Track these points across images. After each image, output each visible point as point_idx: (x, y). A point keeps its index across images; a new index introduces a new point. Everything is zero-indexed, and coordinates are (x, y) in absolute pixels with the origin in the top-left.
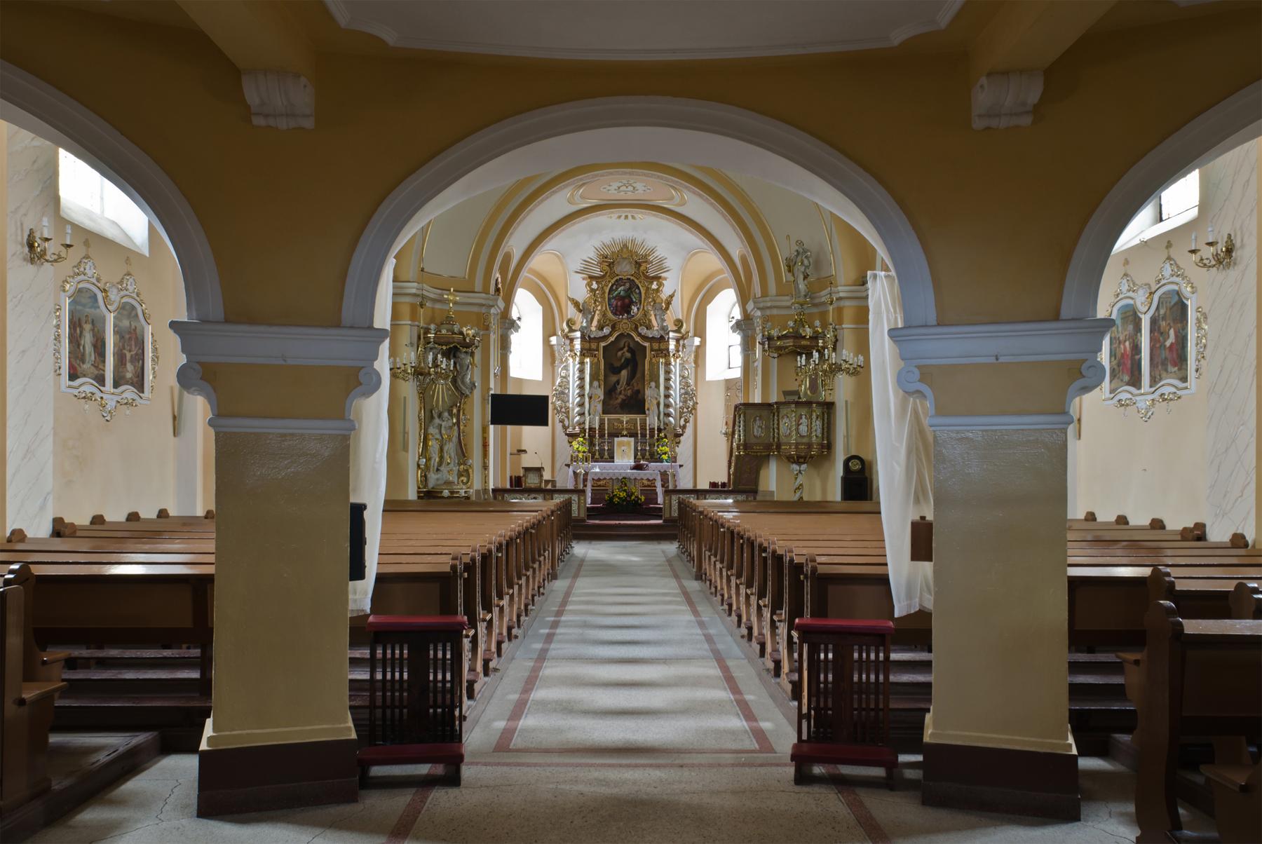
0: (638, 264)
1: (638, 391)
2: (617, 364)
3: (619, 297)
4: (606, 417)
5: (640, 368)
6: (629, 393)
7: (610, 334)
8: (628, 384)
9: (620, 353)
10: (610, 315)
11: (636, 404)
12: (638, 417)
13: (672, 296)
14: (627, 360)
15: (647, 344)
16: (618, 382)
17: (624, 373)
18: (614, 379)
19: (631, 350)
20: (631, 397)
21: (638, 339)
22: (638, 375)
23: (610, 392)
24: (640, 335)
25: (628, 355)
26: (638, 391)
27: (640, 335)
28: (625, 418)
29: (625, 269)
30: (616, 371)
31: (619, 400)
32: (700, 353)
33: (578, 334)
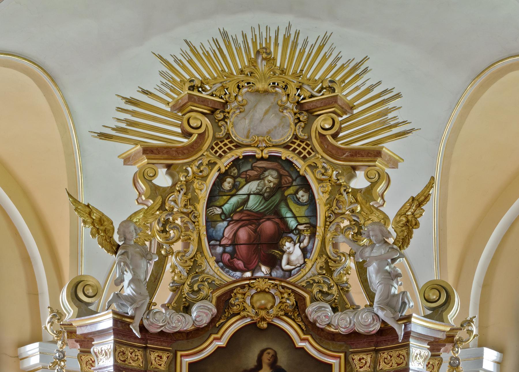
0: (306, 111)
13: (419, 201)
24: (311, 328)
27: (311, 328)
33: (105, 321)
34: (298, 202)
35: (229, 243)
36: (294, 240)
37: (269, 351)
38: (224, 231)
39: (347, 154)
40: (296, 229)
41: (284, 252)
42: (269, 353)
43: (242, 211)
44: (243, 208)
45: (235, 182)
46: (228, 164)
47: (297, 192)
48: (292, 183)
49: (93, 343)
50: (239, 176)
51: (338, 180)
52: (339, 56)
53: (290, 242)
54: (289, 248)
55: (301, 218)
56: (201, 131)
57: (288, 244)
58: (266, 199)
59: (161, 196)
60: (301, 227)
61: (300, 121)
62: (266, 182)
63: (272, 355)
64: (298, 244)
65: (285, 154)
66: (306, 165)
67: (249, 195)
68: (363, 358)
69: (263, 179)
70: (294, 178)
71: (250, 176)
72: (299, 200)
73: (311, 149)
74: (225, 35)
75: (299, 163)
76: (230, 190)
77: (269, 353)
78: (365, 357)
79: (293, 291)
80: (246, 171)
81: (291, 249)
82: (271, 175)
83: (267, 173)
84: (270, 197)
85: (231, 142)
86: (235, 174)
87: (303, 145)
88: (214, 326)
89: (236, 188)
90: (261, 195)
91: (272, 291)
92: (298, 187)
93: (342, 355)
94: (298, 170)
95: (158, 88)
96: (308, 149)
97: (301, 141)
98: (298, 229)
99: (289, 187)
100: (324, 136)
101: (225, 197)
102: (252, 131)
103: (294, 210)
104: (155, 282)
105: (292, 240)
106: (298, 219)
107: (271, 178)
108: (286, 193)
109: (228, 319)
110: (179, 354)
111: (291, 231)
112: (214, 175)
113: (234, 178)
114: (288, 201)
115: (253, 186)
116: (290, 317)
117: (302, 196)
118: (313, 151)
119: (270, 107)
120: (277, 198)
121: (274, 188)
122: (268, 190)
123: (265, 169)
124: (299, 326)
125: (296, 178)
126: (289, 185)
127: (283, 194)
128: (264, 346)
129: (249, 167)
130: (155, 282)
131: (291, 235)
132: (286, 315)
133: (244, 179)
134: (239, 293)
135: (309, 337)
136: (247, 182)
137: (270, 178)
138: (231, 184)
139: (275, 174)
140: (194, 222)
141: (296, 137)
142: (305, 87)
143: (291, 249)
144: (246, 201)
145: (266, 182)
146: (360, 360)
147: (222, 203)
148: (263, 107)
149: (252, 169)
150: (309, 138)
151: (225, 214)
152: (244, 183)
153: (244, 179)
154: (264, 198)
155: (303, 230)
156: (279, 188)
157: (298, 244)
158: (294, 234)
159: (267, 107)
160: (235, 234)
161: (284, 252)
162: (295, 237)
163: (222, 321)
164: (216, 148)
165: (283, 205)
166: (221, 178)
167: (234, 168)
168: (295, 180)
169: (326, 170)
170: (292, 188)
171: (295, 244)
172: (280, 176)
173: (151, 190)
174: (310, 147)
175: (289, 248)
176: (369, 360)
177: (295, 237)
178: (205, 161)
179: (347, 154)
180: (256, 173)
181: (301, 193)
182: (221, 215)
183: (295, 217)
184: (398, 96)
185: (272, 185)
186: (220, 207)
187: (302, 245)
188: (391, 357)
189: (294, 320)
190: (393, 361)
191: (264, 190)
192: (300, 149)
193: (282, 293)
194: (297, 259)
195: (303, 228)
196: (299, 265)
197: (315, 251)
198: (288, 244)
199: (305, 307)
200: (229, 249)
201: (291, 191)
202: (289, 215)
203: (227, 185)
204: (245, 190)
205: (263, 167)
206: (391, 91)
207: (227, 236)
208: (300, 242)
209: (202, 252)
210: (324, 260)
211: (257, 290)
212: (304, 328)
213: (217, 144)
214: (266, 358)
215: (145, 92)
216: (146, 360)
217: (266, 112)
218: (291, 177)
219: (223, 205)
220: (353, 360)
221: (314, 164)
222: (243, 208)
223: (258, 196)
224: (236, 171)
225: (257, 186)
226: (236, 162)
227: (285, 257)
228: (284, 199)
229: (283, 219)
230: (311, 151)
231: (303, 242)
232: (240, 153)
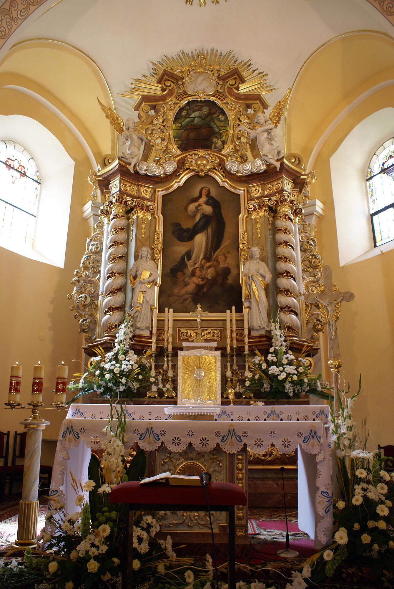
0: (223, 79)
1: (227, 271)
2: (188, 225)
3: (191, 128)
4: (170, 315)
5: (228, 230)
6: (210, 273)
7: (175, 174)
8: (208, 258)
9: (192, 207)
10: (175, 150)
11: (225, 293)
12: (230, 316)
14: (204, 216)
15: (241, 191)
16: (189, 255)
17: (200, 239)
18: (181, 249)
19: (212, 202)
20: (213, 282)
21: (226, 184)
22: (226, 242)
23: (173, 272)
24: (228, 174)
25: (208, 209)
26: (227, 271)
27: (228, 174)
28: (199, 314)
29: (202, 88)
30: (187, 235)
31: (191, 287)
32: (328, 220)
34: (219, 120)
41: (212, 143)
47: (219, 116)
50: (190, 109)
56: (170, 88)
57: (214, 139)
58: (203, 119)
60: (221, 132)
65: (212, 99)
67: (195, 117)
69: (202, 111)
74: (183, 52)
75: (219, 103)
79: (218, 156)
83: (203, 108)
89: (188, 115)
91: (207, 157)
93: (245, 189)
99: (214, 114)
107: (206, 110)
108: (213, 117)
109: (184, 171)
110: (157, 190)
111: (216, 133)
112: (177, 109)
113: (187, 110)
115: (197, 114)
116: (216, 170)
120: (209, 118)
123: (203, 106)
127: (212, 117)
128: (203, 186)
132: (214, 169)
136: (194, 112)
137: (205, 110)
139: (208, 108)
141: (218, 92)
142: (221, 70)
144: (193, 120)
148: (201, 78)
149: (196, 106)
150: (224, 91)
156: (210, 114)
160: (188, 135)
161: (212, 143)
162: (219, 137)
165: (212, 121)
166: (181, 110)
169: (232, 105)
172: (210, 109)
176: (260, 190)
177: (219, 137)
178: (173, 102)
181: (221, 116)
183: (218, 127)
184: (266, 75)
186: (180, 123)
189: (219, 172)
198: (214, 139)
199: (224, 163)
200: (185, 142)
201: (216, 115)
203: (184, 113)
204: (193, 115)
206: (263, 72)
208: (221, 138)
209: (171, 143)
213: (179, 96)
214: (204, 192)
215: (144, 76)
216: (139, 191)
217: (203, 80)
226: (189, 103)
227: (213, 145)
228: (212, 119)
229: (212, 128)
232: (190, 99)
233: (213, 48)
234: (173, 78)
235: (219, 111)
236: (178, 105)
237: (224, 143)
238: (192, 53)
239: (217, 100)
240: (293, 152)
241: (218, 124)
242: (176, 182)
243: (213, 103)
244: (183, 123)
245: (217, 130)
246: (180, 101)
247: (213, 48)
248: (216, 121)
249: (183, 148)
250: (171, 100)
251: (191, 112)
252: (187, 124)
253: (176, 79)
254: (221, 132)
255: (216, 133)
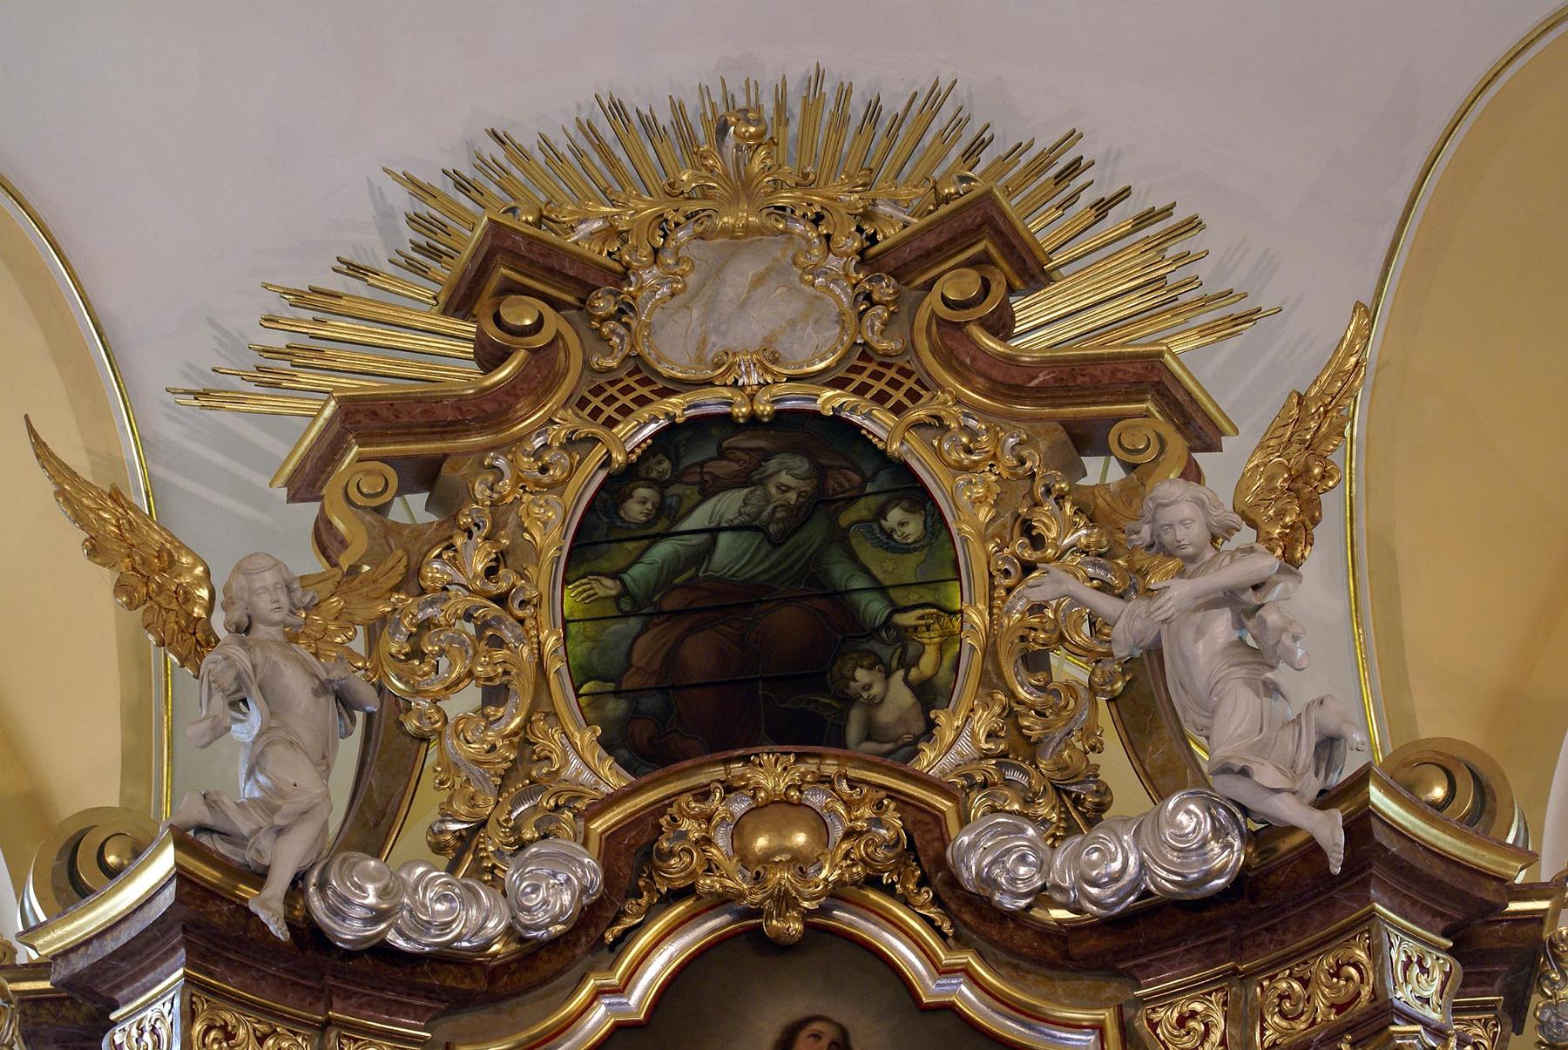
0: (894, 266)
10: (583, 760)
24: (972, 915)
27: (972, 915)
29: (755, 330)
34: (890, 543)
35: (652, 683)
36: (886, 658)
37: (816, 1027)
38: (631, 648)
39: (1041, 377)
40: (888, 624)
41: (850, 701)
42: (817, 1036)
43: (688, 586)
44: (696, 574)
45: (663, 497)
46: (638, 446)
47: (882, 513)
48: (862, 486)
49: (113, 1017)
50: (677, 478)
51: (1022, 462)
52: (986, 136)
53: (870, 668)
54: (868, 687)
55: (902, 592)
56: (539, 340)
57: (862, 675)
58: (776, 544)
59: (407, 552)
60: (908, 619)
61: (873, 304)
62: (773, 491)
63: (832, 1043)
64: (900, 674)
65: (828, 400)
66: (903, 425)
67: (714, 532)
68: (1193, 1014)
70: (869, 473)
71: (716, 478)
72: (890, 536)
73: (918, 382)
75: (878, 424)
76: (649, 523)
77: (817, 1036)
78: (1198, 1007)
79: (893, 794)
80: (702, 464)
81: (877, 689)
82: (789, 471)
83: (772, 465)
84: (786, 536)
85: (644, 382)
86: (662, 473)
87: (891, 374)
88: (593, 934)
89: (666, 515)
90: (757, 529)
91: (817, 800)
92: (882, 498)
93: (1107, 1015)
94: (880, 445)
95: (402, 260)
96: (909, 384)
97: (881, 364)
98: (897, 627)
99: (852, 500)
100: (959, 326)
101: (631, 546)
102: (713, 338)
103: (876, 571)
104: (376, 825)
105: (879, 661)
106: (893, 593)
107: (788, 478)
108: (845, 519)
109: (651, 913)
111: (874, 633)
112: (588, 477)
113: (661, 485)
114: (853, 542)
115: (728, 505)
116: (889, 890)
117: (902, 524)
118: (927, 389)
119: (770, 270)
120: (815, 533)
121: (799, 506)
122: (779, 515)
123: (767, 455)
124: (928, 921)
125: (875, 474)
126: (854, 493)
128: (797, 1008)
129: (711, 451)
130: (376, 825)
131: (875, 646)
132: (873, 882)
133: (696, 488)
134: (690, 817)
135: (970, 959)
136: (706, 495)
137: (784, 478)
138: (649, 506)
140: (521, 621)
141: (867, 352)
142: (884, 209)
143: (877, 689)
145: (773, 491)
146: (1182, 1022)
147: (621, 563)
148: (744, 270)
149: (722, 455)
150: (912, 347)
151: (634, 598)
152: (697, 497)
153: (696, 488)
154: (767, 536)
155: (916, 628)
156: (820, 503)
157: (900, 674)
158: (882, 641)
159: (762, 268)
161: (850, 701)
162: (889, 654)
163: (629, 922)
164: (596, 402)
166: (617, 484)
167: (660, 457)
168: (872, 479)
169: (973, 434)
170: (863, 501)
171: (888, 674)
173: (371, 537)
174: (914, 378)
175: (868, 687)
176: (1218, 1018)
177: (889, 654)
178: (559, 433)
179: (1041, 377)
180: (735, 467)
181: (895, 515)
182: (617, 599)
183: (881, 589)
185: (792, 497)
186: (615, 575)
187: (914, 673)
188: (1305, 983)
189: (906, 902)
190: (1321, 1003)
191: (765, 514)
192: (879, 386)
193: (848, 805)
194: (901, 720)
195: (914, 622)
196: (907, 738)
197: (969, 666)
198: (862, 675)
199: (944, 840)
200: (650, 703)
201: (861, 510)
202: (859, 583)
203: (637, 506)
204: (700, 518)
205: (761, 449)
206: (1167, 212)
207: (642, 664)
208: (907, 664)
209: (552, 715)
210: (997, 709)
211: (754, 797)
212: (946, 927)
213: (596, 391)
215: (355, 270)
217: (759, 280)
218: (857, 470)
219: (625, 570)
220: (1154, 1026)
221: (933, 421)
222: (696, 574)
223: (745, 534)
224: (666, 465)
225: (740, 503)
226: (668, 439)
227: (856, 717)
228: (840, 538)
229: (839, 598)
230: (916, 387)
231: (916, 664)
232: (676, 406)
233: (820, 75)
234: (553, 274)
235: (884, 480)
236: (599, 453)
237: (929, 695)
238: (678, 109)
239: (865, 404)
240: (1429, 728)
241: (884, 567)
242: (599, 993)
243: (840, 429)
244: (637, 570)
245: (875, 608)
246: (611, 423)
247: (820, 75)
248: (867, 553)
249: (643, 745)
250: (546, 424)
251: (691, 492)
252: (665, 581)
253: (576, 283)
254: (908, 619)
255: (874, 633)
